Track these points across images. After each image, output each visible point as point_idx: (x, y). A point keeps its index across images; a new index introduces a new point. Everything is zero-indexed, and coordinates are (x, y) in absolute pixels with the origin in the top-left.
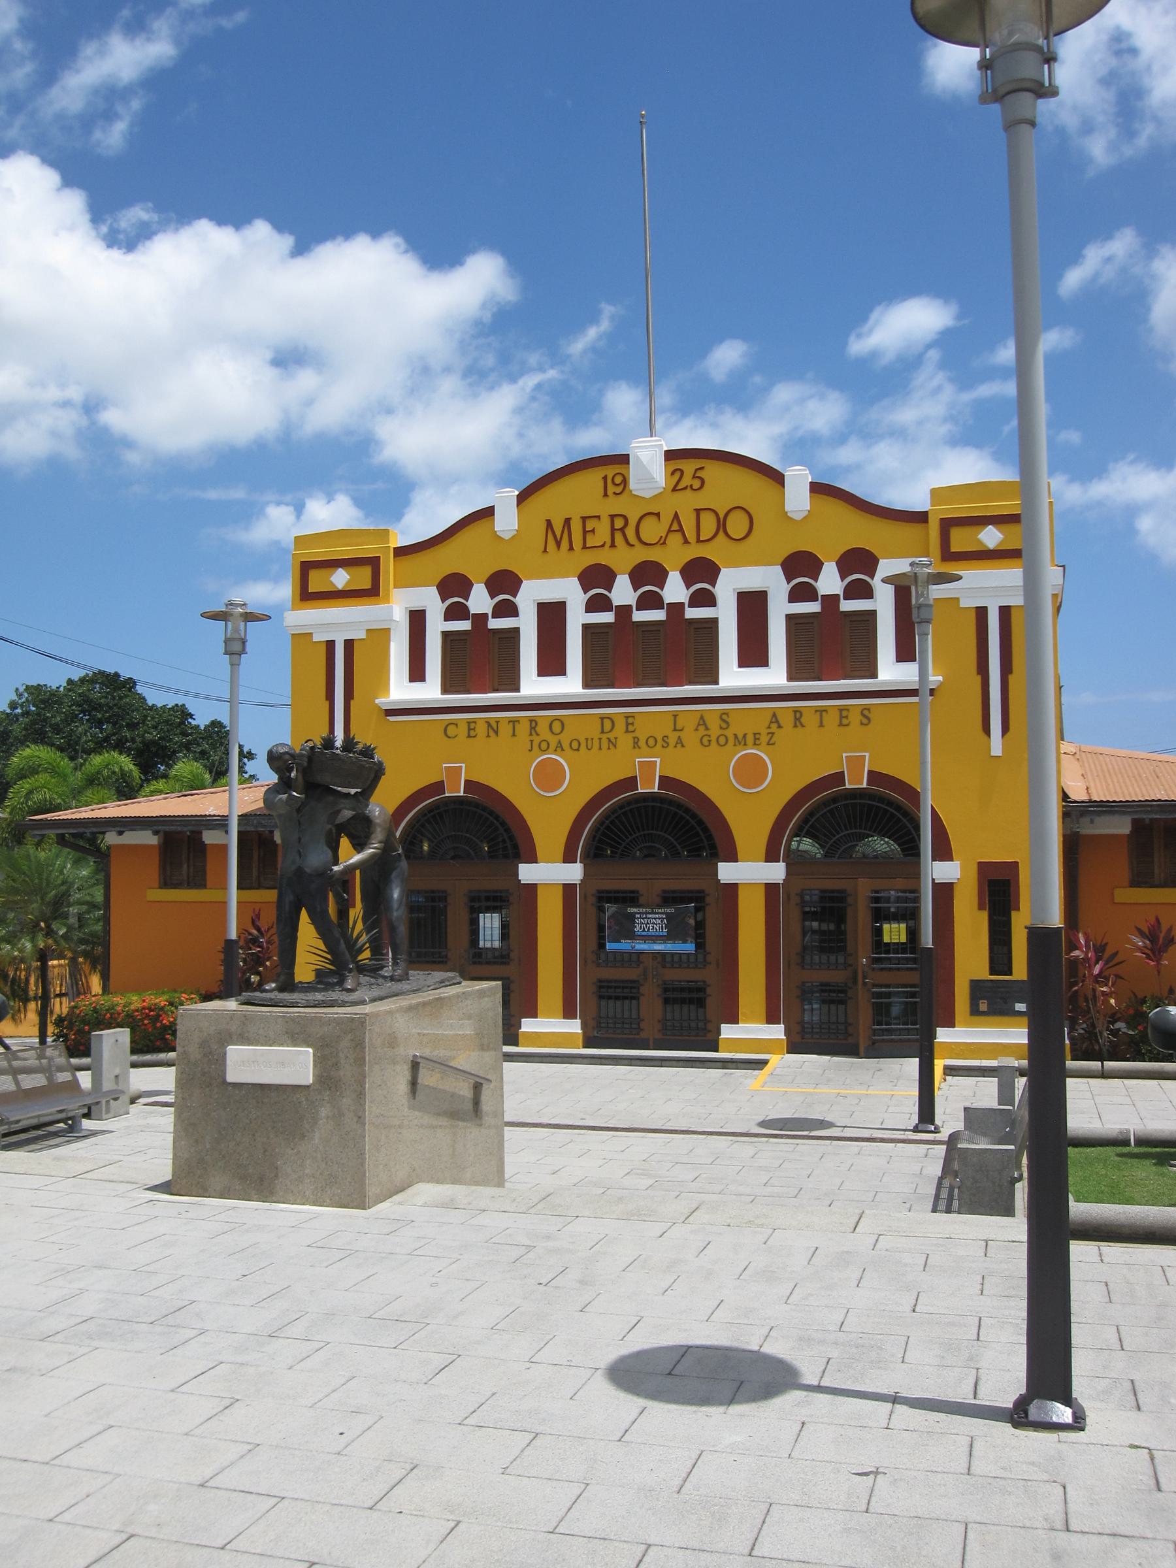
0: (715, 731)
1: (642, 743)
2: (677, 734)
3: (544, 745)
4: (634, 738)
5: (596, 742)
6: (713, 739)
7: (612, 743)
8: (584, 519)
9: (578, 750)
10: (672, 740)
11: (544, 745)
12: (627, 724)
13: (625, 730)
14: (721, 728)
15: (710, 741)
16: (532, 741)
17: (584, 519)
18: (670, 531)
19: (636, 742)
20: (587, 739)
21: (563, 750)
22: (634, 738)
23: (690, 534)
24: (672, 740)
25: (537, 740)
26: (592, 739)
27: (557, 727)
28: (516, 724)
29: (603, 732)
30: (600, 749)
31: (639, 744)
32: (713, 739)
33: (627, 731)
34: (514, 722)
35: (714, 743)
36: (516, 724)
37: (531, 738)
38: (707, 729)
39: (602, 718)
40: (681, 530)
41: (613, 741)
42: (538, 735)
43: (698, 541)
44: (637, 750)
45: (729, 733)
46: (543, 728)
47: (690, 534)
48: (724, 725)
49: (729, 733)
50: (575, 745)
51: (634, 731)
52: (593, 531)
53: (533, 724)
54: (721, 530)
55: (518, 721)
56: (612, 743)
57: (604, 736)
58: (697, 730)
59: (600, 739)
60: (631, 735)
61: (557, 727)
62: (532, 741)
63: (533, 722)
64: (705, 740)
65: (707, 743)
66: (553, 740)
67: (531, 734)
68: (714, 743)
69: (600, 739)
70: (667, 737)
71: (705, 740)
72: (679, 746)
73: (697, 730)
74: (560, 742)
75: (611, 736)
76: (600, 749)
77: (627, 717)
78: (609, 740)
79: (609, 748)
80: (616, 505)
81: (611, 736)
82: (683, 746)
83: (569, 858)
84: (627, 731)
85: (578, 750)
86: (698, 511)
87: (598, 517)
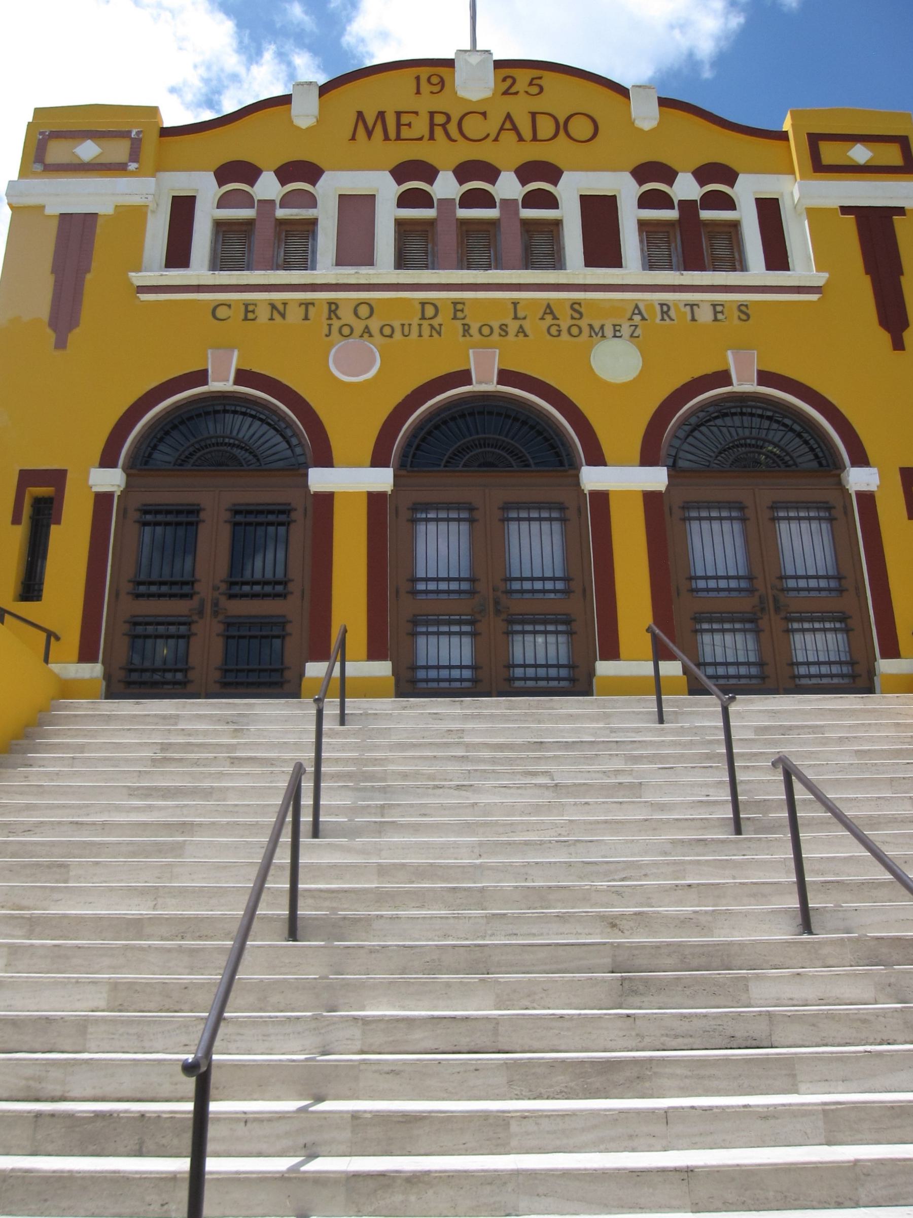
0: (565, 324)
1: (474, 330)
2: (517, 324)
3: (346, 331)
4: (464, 325)
5: (415, 329)
6: (564, 327)
7: (436, 331)
8: (398, 114)
9: (391, 336)
10: (513, 326)
11: (346, 331)
12: (456, 311)
13: (452, 316)
14: (573, 318)
15: (559, 331)
16: (330, 325)
17: (398, 114)
18: (502, 129)
19: (466, 330)
20: (403, 325)
21: (371, 336)
22: (464, 325)
23: (527, 133)
24: (513, 326)
25: (336, 324)
26: (410, 325)
27: (364, 311)
28: (310, 307)
29: (423, 318)
30: (420, 336)
31: (472, 331)
32: (564, 327)
33: (455, 318)
34: (307, 304)
35: (564, 334)
36: (310, 307)
37: (330, 322)
38: (555, 318)
39: (423, 304)
40: (515, 128)
41: (437, 328)
42: (339, 318)
43: (535, 139)
44: (468, 338)
45: (583, 323)
46: (346, 314)
47: (527, 133)
48: (576, 315)
49: (583, 323)
50: (387, 331)
51: (463, 319)
52: (409, 125)
53: (333, 307)
54: (562, 132)
55: (313, 304)
56: (436, 331)
57: (425, 323)
58: (542, 318)
59: (420, 325)
60: (458, 323)
61: (364, 311)
62: (330, 325)
63: (333, 308)
64: (554, 330)
65: (555, 333)
66: (359, 326)
67: (330, 318)
68: (564, 334)
69: (420, 325)
70: (506, 326)
71: (554, 330)
72: (521, 335)
73: (542, 318)
74: (367, 327)
75: (435, 322)
76: (420, 336)
77: (455, 303)
78: (432, 327)
79: (431, 336)
80: (439, 103)
81: (435, 322)
82: (526, 336)
83: (378, 460)
84: (455, 318)
85: (391, 336)
86: (534, 115)
87: (416, 113)
